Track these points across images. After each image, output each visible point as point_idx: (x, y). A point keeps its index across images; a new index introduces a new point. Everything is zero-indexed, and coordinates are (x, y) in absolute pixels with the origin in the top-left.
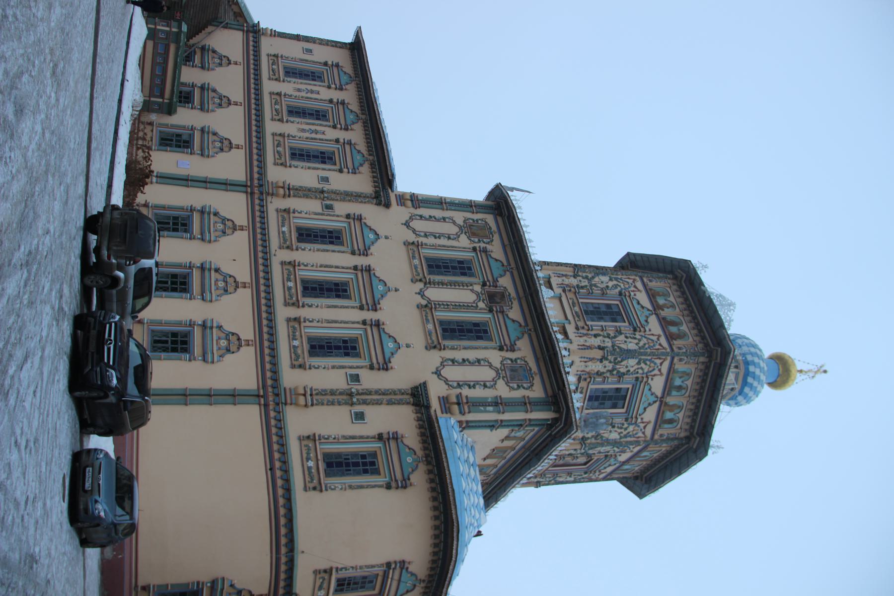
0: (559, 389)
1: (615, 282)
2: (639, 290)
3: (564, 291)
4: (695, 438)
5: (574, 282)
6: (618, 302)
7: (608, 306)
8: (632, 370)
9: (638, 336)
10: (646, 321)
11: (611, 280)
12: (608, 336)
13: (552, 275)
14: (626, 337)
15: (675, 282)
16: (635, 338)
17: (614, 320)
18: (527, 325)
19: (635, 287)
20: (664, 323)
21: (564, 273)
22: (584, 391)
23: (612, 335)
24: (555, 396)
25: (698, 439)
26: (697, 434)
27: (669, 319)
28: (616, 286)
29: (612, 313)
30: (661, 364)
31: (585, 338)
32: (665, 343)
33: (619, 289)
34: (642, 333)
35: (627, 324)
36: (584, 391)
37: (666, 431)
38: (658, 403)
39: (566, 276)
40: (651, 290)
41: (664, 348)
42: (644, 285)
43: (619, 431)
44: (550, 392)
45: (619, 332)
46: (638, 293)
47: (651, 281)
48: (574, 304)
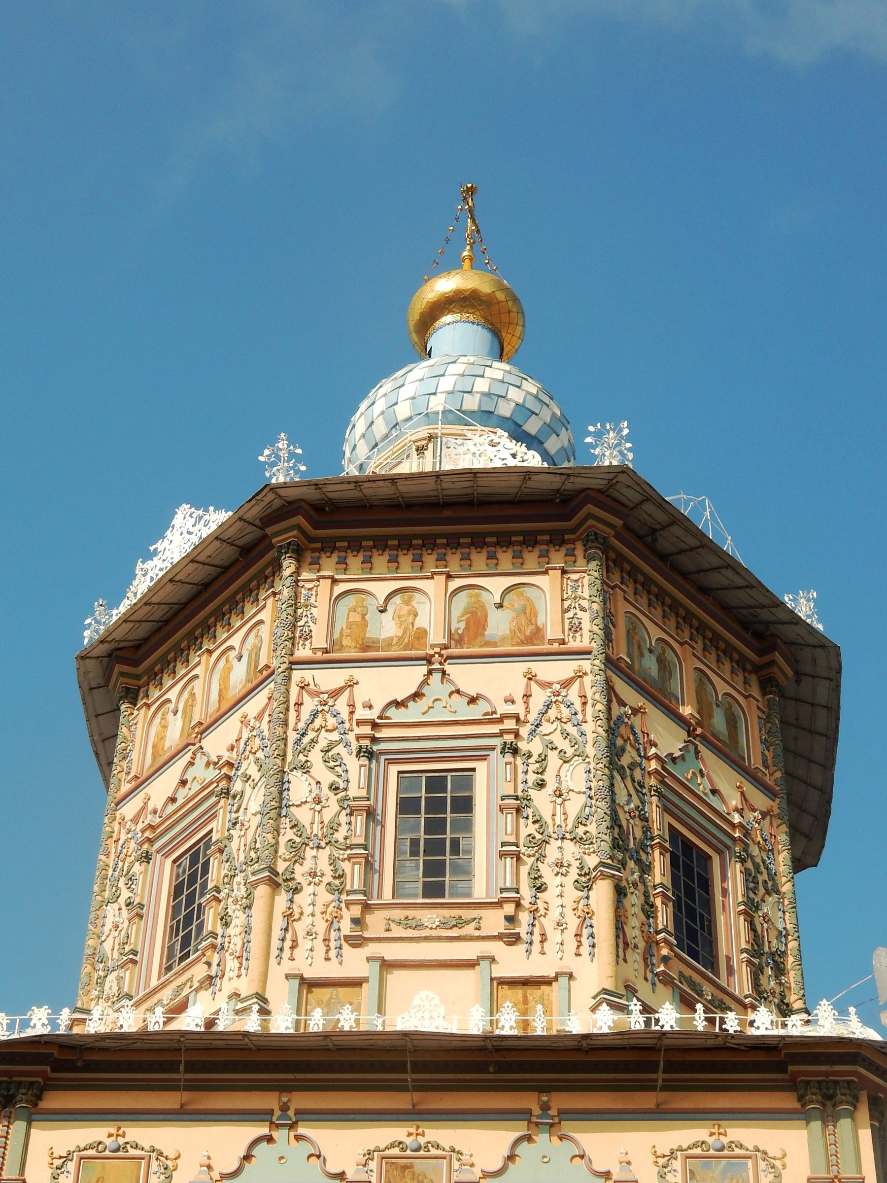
0: (780, 1067)
1: (315, 756)
2: (351, 684)
3: (357, 942)
4: (773, 663)
5: (313, 899)
6: (394, 770)
7: (406, 806)
8: (635, 802)
9: (536, 747)
10: (473, 700)
11: (305, 768)
12: (539, 844)
13: (287, 966)
14: (541, 785)
15: (308, 556)
16: (542, 759)
17: (465, 805)
18: (524, 1114)
19: (335, 694)
20: (469, 642)
21: (279, 922)
22: (688, 972)
23: (532, 829)
24: (798, 1087)
25: (777, 656)
26: (760, 653)
27: (459, 626)
28: (333, 762)
29: (436, 805)
30: (622, 704)
31: (548, 923)
32: (562, 669)
33: (340, 749)
34: (524, 731)
35: (481, 767)
36: (688, 972)
37: (753, 745)
38: (701, 747)
39: (289, 916)
40: (334, 644)
41: (580, 675)
42: (327, 660)
43: (762, 891)
44: (788, 1101)
45: (519, 806)
46: (361, 694)
47: (308, 636)
48: (406, 923)
